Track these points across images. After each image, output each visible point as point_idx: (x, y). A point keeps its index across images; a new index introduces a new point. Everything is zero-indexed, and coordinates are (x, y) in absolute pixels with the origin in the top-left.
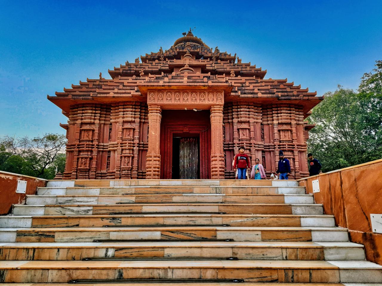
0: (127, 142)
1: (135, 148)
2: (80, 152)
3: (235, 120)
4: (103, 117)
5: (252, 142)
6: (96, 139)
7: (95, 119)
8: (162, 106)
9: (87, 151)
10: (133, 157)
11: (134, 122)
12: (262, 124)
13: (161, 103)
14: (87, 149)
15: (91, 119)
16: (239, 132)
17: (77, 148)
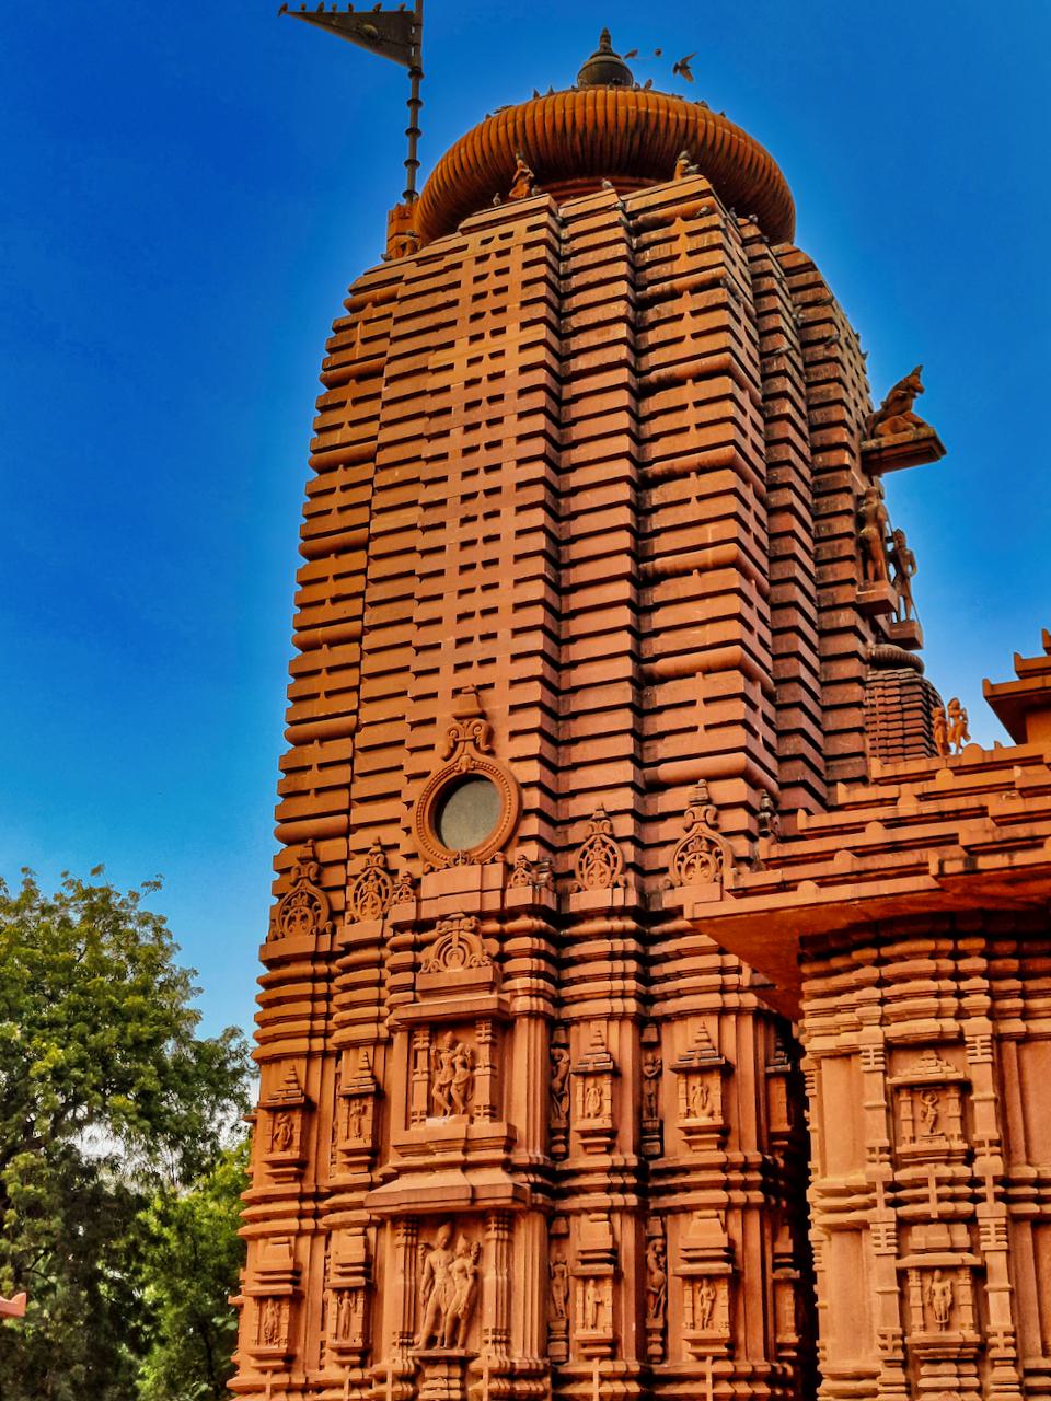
2: (904, 1225)
4: (1007, 994)
6: (991, 1143)
9: (948, 1220)
14: (948, 1207)
15: (939, 1014)
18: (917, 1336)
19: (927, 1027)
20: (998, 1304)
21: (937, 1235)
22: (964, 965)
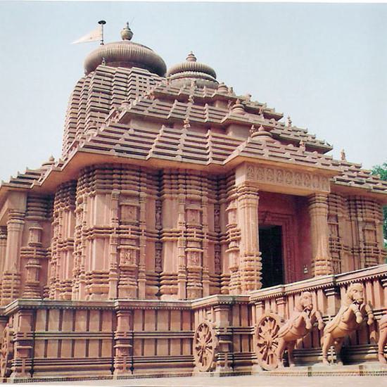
5: (341, 242)
13: (261, 182)
17: (117, 233)
18: (121, 264)
20: (142, 259)
22: (142, 179)
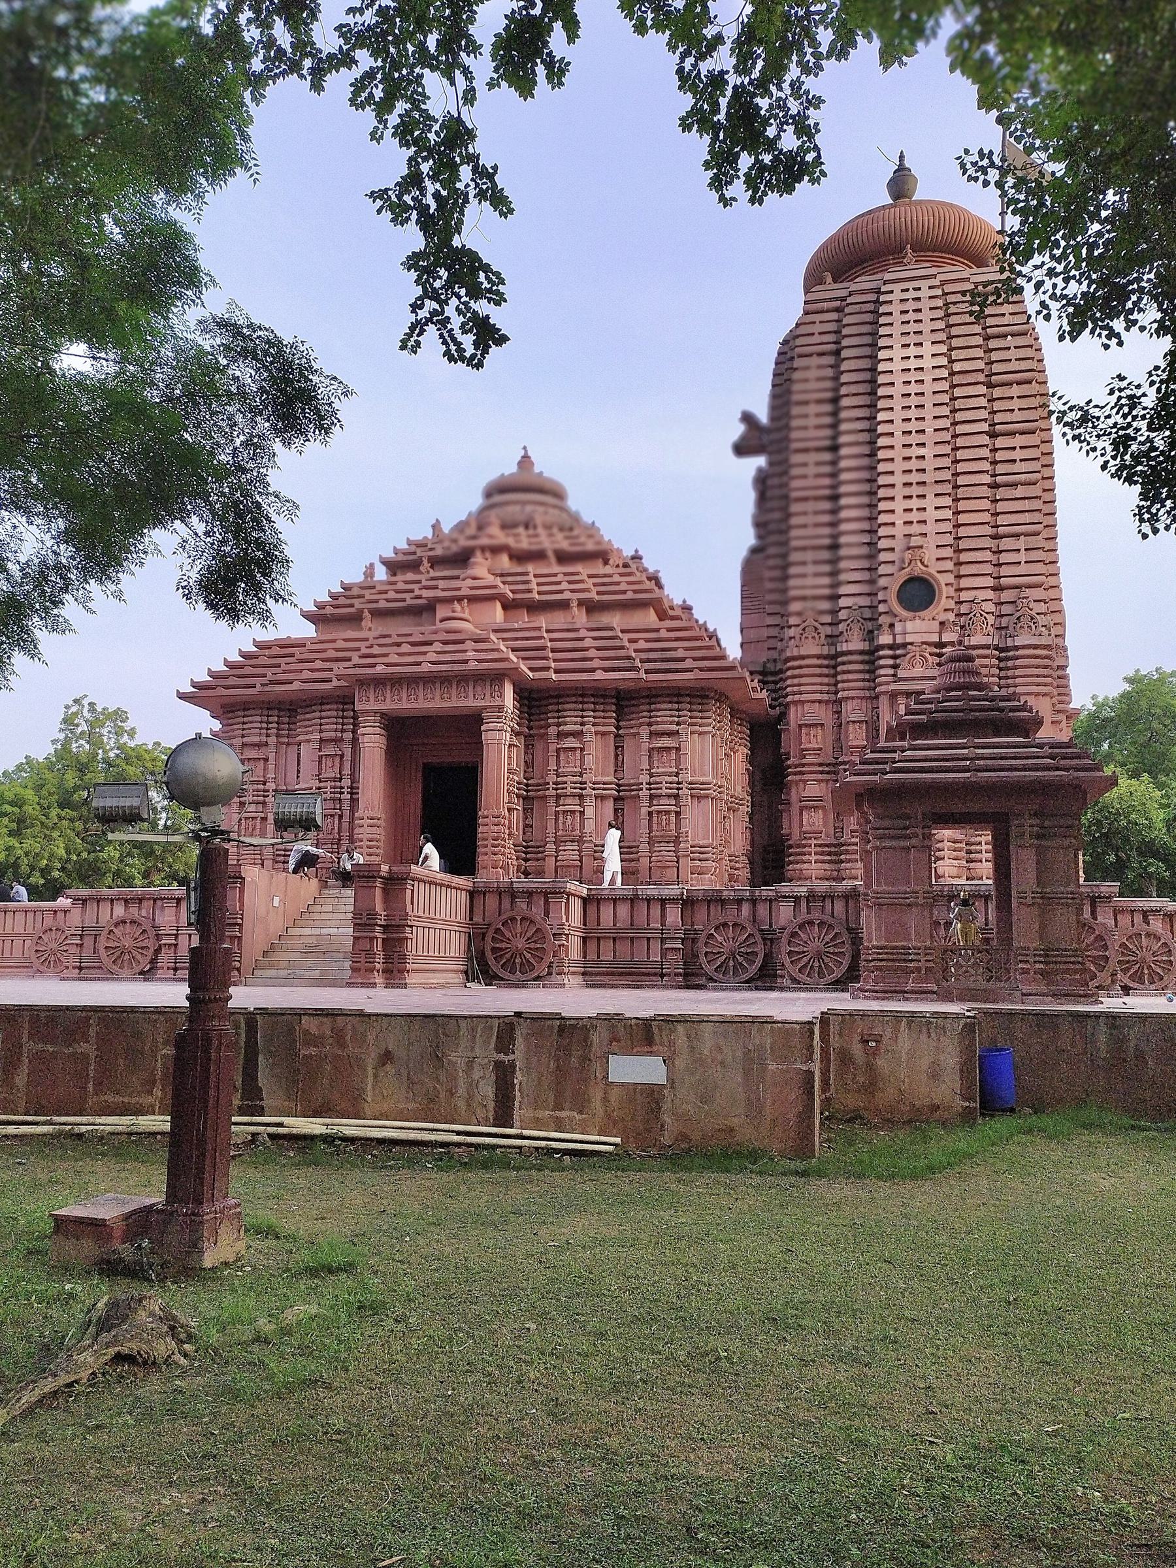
0: (329, 784)
1: (343, 797)
3: (552, 730)
7: (268, 735)
8: (383, 715)
10: (341, 817)
11: (341, 740)
12: (617, 736)
16: (558, 756)
19: (256, 739)
21: (253, 808)
